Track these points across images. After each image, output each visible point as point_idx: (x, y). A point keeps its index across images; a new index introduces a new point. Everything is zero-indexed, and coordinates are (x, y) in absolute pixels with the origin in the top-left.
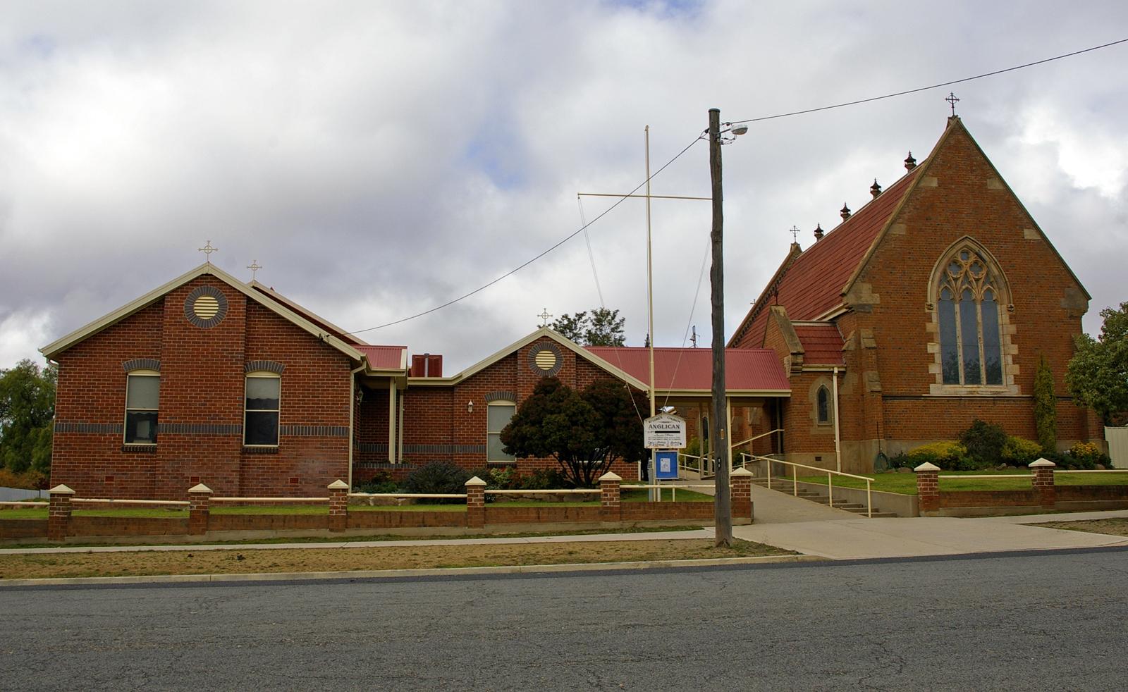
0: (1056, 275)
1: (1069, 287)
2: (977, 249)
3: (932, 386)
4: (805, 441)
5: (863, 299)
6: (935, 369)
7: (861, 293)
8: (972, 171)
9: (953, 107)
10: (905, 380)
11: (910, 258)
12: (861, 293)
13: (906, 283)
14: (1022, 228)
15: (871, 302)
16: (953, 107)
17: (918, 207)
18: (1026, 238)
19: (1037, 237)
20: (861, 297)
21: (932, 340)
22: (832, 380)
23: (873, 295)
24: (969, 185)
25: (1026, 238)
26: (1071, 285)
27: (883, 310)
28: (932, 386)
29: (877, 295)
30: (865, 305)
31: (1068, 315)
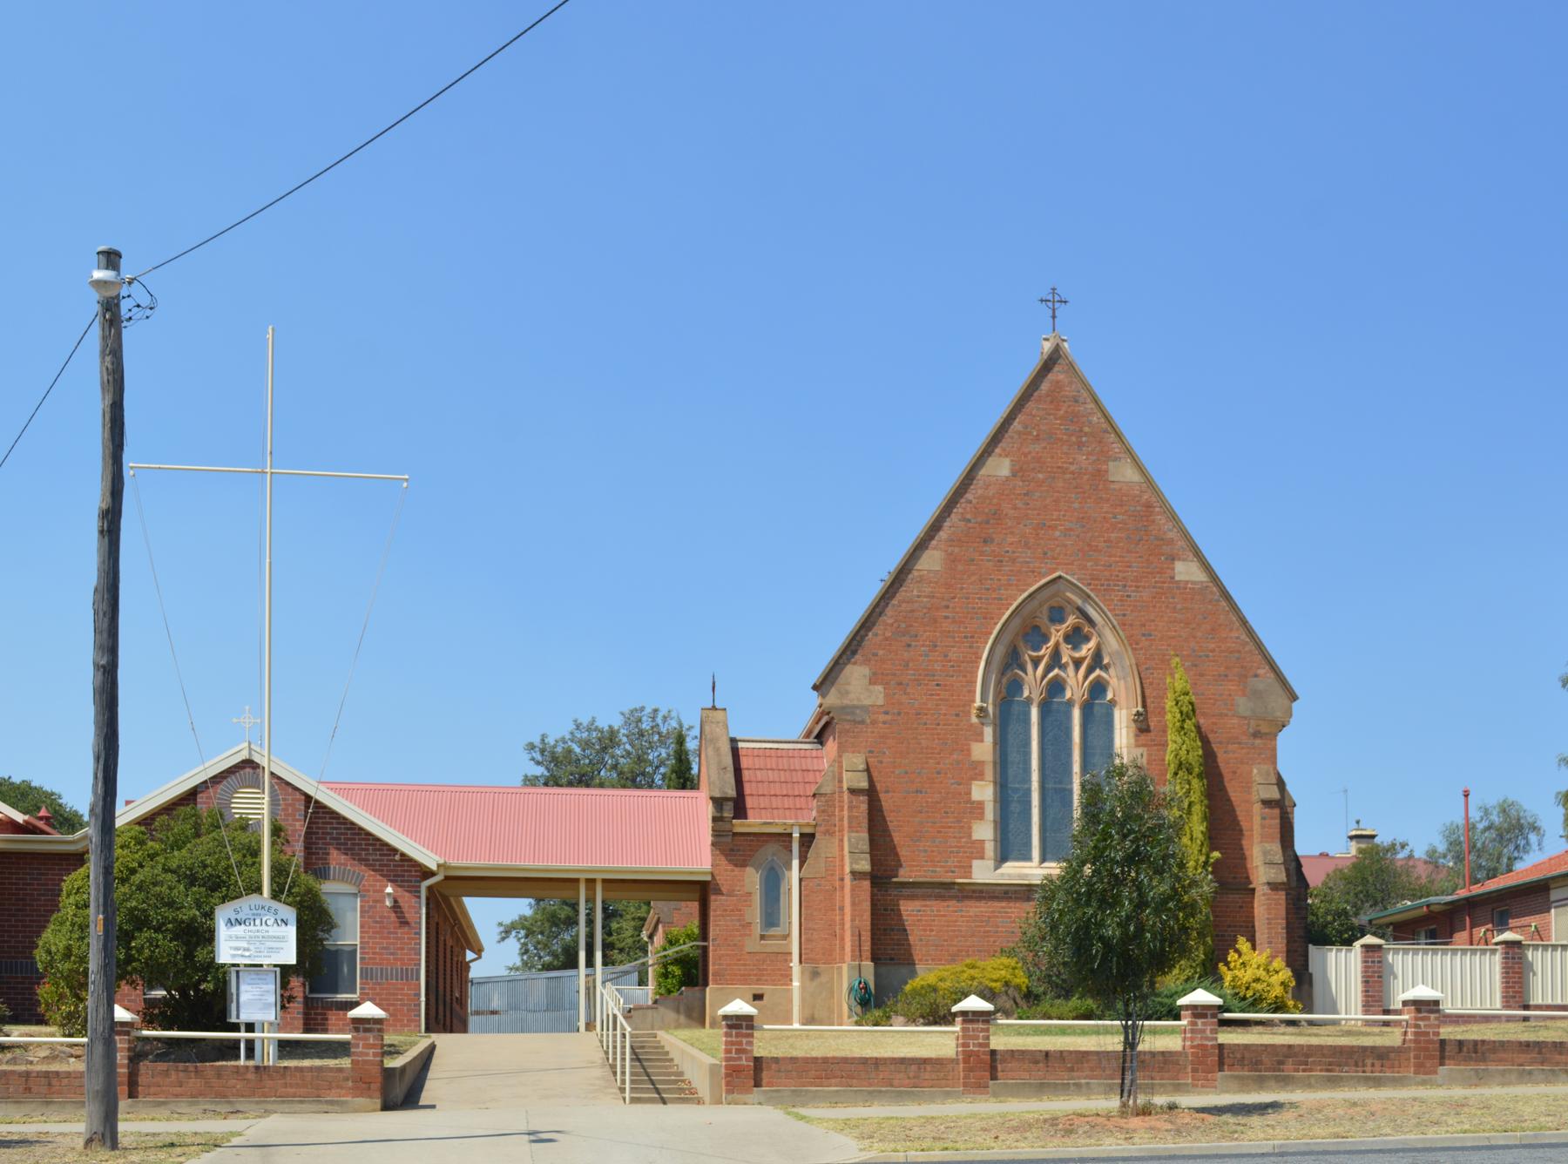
0: (1231, 652)
1: (1256, 676)
2: (1079, 602)
3: (976, 863)
4: (736, 965)
5: (852, 696)
6: (984, 831)
7: (849, 684)
8: (1080, 445)
9: (1054, 317)
10: (925, 851)
11: (946, 617)
12: (849, 684)
13: (937, 667)
14: (1172, 558)
15: (867, 702)
16: (1054, 317)
17: (968, 516)
18: (1177, 578)
19: (1199, 576)
20: (847, 693)
21: (980, 776)
22: (791, 851)
23: (871, 687)
24: (1073, 473)
25: (1177, 578)
26: (1261, 672)
27: (888, 717)
28: (976, 863)
29: (880, 688)
31: (1251, 730)
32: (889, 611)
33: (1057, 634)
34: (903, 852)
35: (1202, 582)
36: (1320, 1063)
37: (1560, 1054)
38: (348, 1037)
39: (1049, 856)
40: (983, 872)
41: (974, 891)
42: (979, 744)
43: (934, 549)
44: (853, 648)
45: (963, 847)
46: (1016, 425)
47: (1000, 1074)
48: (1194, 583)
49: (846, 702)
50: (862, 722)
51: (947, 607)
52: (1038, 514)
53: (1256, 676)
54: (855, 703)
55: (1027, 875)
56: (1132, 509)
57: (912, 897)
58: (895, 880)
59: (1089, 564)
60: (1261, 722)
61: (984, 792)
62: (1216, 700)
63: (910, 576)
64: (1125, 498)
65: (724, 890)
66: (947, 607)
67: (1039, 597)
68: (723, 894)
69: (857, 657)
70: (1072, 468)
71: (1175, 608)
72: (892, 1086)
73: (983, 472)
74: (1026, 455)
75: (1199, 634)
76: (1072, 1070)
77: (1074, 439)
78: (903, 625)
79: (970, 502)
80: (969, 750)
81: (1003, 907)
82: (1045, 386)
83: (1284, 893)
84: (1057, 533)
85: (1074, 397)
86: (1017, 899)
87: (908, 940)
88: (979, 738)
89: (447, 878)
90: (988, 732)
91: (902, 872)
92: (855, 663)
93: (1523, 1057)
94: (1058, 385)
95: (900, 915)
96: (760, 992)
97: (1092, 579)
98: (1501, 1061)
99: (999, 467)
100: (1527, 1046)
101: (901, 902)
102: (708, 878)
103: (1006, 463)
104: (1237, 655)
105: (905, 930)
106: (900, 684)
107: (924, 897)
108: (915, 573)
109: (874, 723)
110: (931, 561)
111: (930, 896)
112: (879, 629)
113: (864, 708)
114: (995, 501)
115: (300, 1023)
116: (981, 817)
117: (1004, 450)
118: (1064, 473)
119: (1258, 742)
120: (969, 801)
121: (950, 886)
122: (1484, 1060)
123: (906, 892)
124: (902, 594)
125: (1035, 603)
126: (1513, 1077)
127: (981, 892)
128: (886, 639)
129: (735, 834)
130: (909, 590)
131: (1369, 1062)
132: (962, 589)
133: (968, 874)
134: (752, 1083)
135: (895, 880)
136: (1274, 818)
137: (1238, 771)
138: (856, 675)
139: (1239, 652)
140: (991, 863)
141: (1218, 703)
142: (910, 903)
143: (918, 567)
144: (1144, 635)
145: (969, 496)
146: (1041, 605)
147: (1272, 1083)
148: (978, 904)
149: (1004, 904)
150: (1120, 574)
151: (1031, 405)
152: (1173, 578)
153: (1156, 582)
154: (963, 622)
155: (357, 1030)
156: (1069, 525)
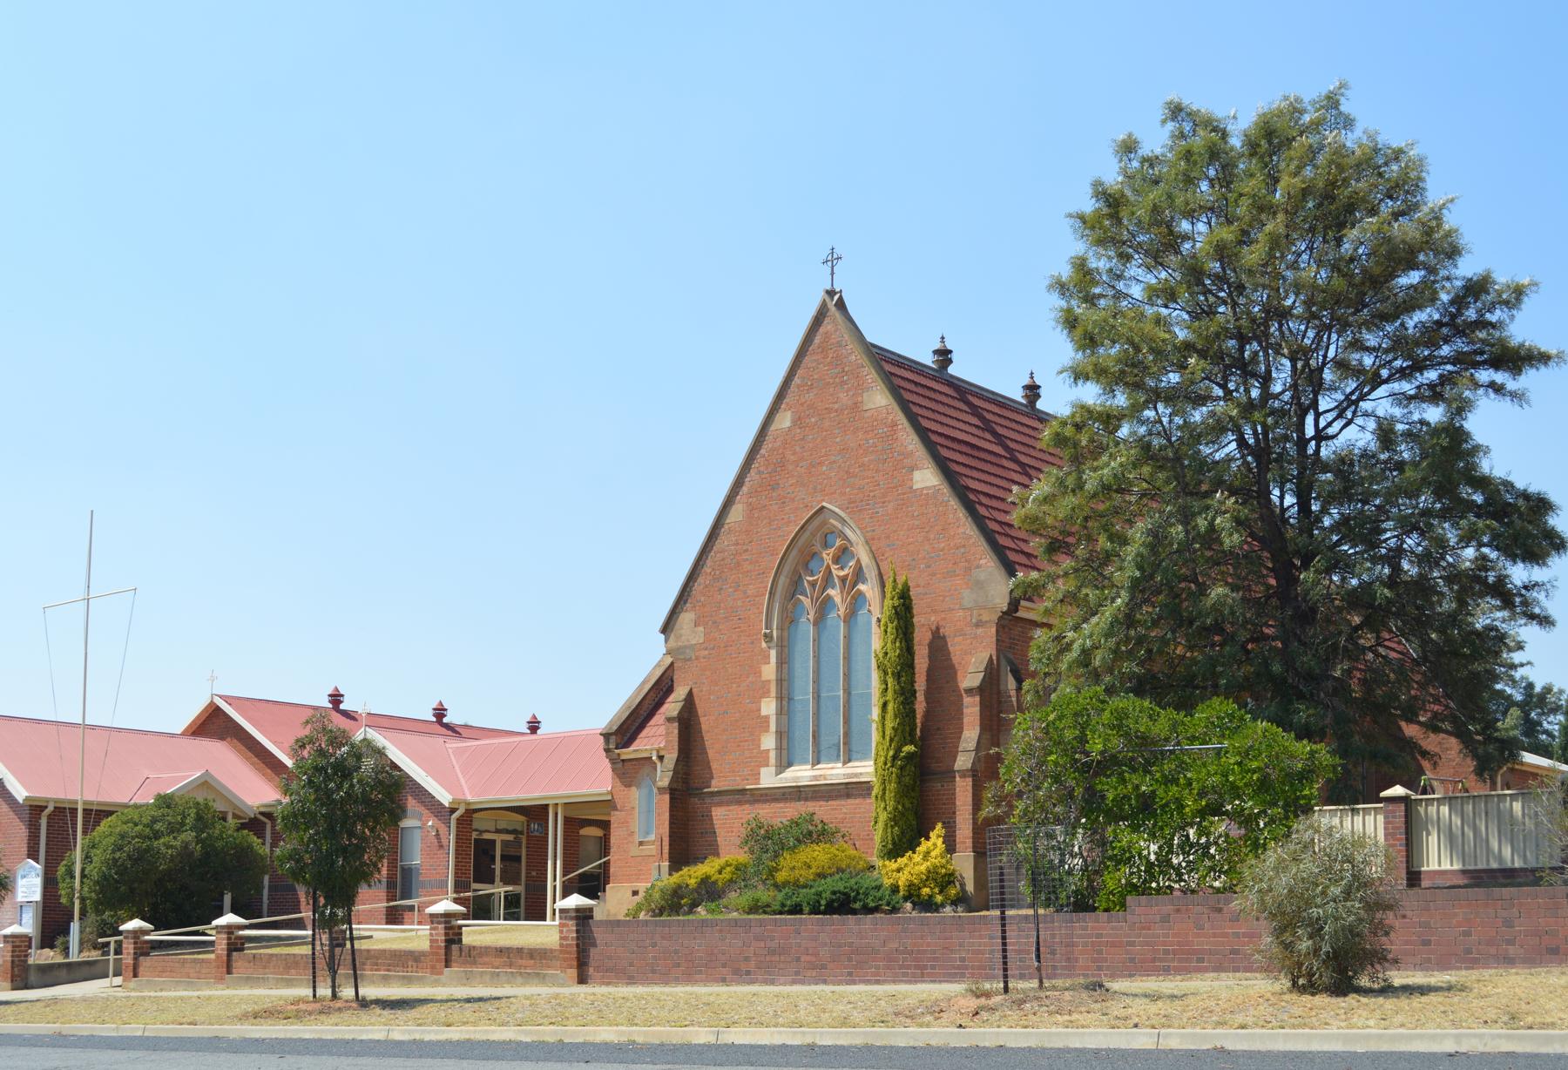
1: (978, 567)
3: (763, 771)
6: (769, 742)
7: (682, 628)
8: (843, 383)
9: (832, 274)
12: (682, 628)
14: (912, 469)
16: (832, 274)
18: (914, 487)
20: (681, 636)
21: (766, 694)
25: (914, 487)
28: (763, 771)
30: (686, 647)
31: (974, 621)
32: (709, 562)
33: (827, 556)
34: (714, 766)
35: (935, 486)
36: (384, 964)
37: (522, 959)
38: (100, 940)
39: (823, 758)
40: (768, 779)
41: (762, 795)
42: (767, 666)
43: (739, 502)
44: (685, 598)
45: (755, 757)
46: (797, 380)
47: (234, 970)
48: (927, 488)
49: (680, 644)
50: (690, 659)
51: (746, 550)
52: (811, 455)
53: (978, 567)
54: (686, 643)
55: (798, 778)
56: (880, 431)
57: (720, 804)
58: (706, 790)
59: (848, 490)
60: (982, 612)
61: (769, 707)
62: (945, 597)
63: (723, 530)
64: (875, 423)
65: (619, 807)
66: (746, 550)
67: (811, 527)
68: (617, 810)
69: (688, 605)
70: (836, 406)
71: (913, 516)
72: (189, 977)
73: (772, 428)
74: (802, 404)
75: (932, 536)
76: (265, 967)
77: (837, 380)
78: (718, 572)
79: (764, 456)
80: (760, 672)
81: (781, 808)
82: (817, 340)
83: (971, 779)
84: (824, 468)
85: (838, 342)
86: (792, 800)
87: (716, 841)
88: (767, 660)
89: (467, 811)
90: (773, 653)
91: (714, 782)
92: (686, 611)
93: (497, 961)
94: (827, 335)
95: (712, 820)
96: (635, 889)
97: (849, 503)
98: (485, 964)
99: (784, 421)
100: (501, 951)
101: (713, 809)
102: (609, 798)
103: (789, 415)
104: (962, 550)
105: (715, 833)
106: (715, 622)
107: (728, 803)
108: (726, 527)
109: (697, 658)
110: (737, 514)
111: (731, 802)
112: (700, 580)
113: (692, 647)
114: (780, 451)
115: (384, 921)
116: (767, 729)
117: (787, 404)
118: (830, 413)
119: (980, 631)
120: (759, 716)
121: (743, 792)
122: (474, 963)
123: (716, 799)
124: (718, 546)
125: (807, 535)
126: (487, 978)
127: (766, 795)
128: (706, 586)
129: (623, 760)
130: (723, 542)
131: (410, 963)
132: (757, 532)
133: (757, 780)
134: (132, 974)
135: (706, 790)
136: (976, 706)
137: (963, 662)
138: (686, 618)
139: (964, 546)
140: (773, 769)
141: (947, 599)
142: (719, 809)
143: (728, 521)
144: (889, 546)
145: (763, 451)
146: (813, 535)
147: (519, 980)
148: (764, 806)
149: (782, 805)
150: (872, 494)
151: (807, 360)
152: (911, 488)
153: (899, 495)
154: (757, 562)
155: (432, 922)
156: (833, 458)
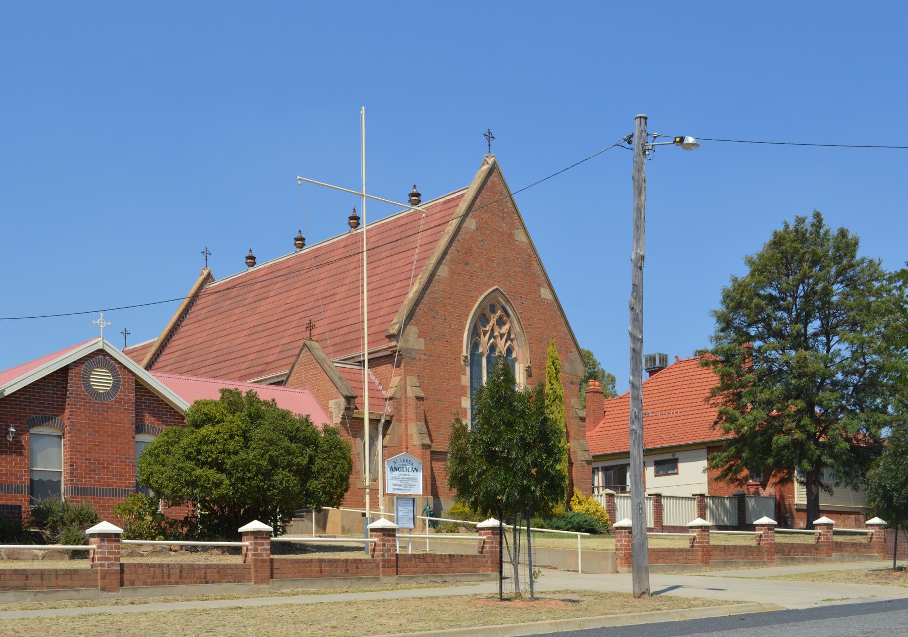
0: (562, 339)
1: (571, 352)
2: (504, 303)
4: (353, 495)
5: (410, 343)
7: (409, 336)
10: (443, 434)
11: (450, 304)
12: (409, 336)
13: (447, 331)
14: (539, 286)
15: (417, 348)
17: (459, 249)
18: (542, 296)
19: (550, 297)
20: (408, 341)
21: (464, 394)
22: (378, 430)
23: (419, 339)
24: (500, 233)
25: (542, 296)
26: (573, 350)
27: (426, 357)
29: (422, 340)
30: (412, 349)
43: (444, 264)
48: (548, 300)
54: (412, 347)
63: (434, 278)
69: (412, 321)
70: (500, 230)
76: (732, 555)
78: (432, 306)
80: (460, 379)
82: (489, 183)
90: (468, 369)
92: (411, 324)
93: (852, 550)
98: (846, 551)
109: (420, 359)
112: (421, 306)
113: (414, 350)
119: (572, 386)
120: (461, 408)
122: (842, 551)
124: (430, 289)
126: (851, 558)
128: (425, 312)
131: (813, 551)
145: (458, 237)
152: (540, 296)
156: (500, 261)
